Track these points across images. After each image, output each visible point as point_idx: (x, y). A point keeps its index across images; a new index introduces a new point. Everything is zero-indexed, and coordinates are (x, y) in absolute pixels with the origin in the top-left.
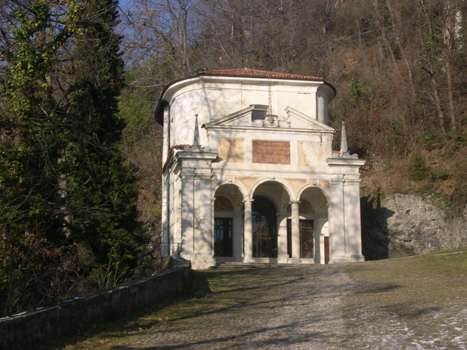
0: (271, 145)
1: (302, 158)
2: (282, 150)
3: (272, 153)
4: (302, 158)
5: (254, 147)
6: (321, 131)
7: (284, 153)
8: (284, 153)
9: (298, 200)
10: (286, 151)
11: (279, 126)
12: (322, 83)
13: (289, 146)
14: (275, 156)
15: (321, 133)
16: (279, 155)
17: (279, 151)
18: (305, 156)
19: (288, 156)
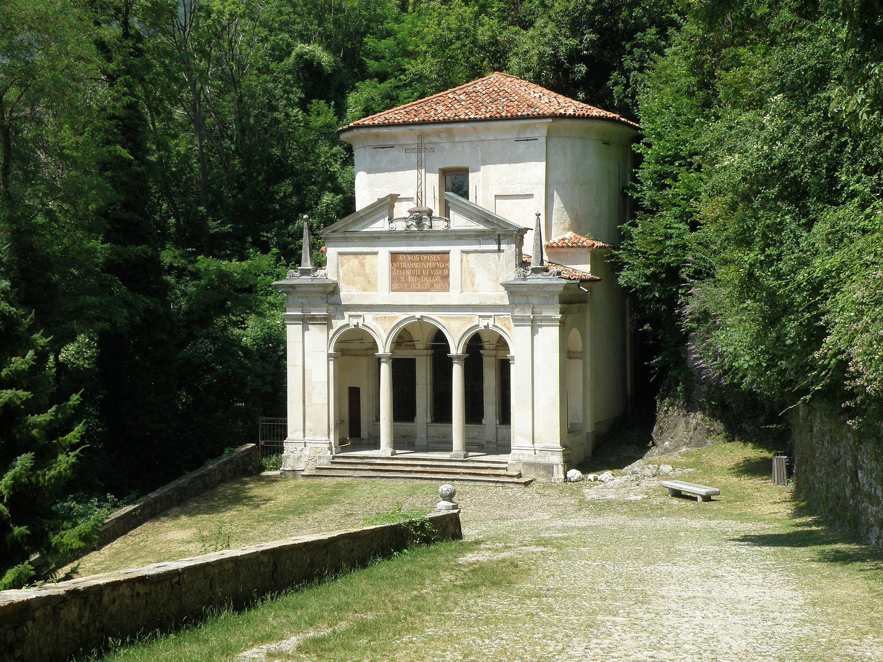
0: (420, 261)
1: (468, 280)
2: (436, 267)
3: (422, 273)
4: (468, 280)
5: (393, 265)
6: (497, 233)
7: (440, 272)
8: (440, 272)
9: (460, 352)
10: (443, 268)
11: (431, 227)
12: (550, 120)
13: (448, 261)
14: (426, 279)
15: (499, 235)
16: (431, 276)
17: (432, 269)
18: (474, 276)
19: (446, 277)
